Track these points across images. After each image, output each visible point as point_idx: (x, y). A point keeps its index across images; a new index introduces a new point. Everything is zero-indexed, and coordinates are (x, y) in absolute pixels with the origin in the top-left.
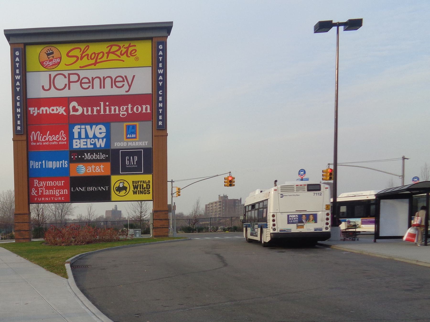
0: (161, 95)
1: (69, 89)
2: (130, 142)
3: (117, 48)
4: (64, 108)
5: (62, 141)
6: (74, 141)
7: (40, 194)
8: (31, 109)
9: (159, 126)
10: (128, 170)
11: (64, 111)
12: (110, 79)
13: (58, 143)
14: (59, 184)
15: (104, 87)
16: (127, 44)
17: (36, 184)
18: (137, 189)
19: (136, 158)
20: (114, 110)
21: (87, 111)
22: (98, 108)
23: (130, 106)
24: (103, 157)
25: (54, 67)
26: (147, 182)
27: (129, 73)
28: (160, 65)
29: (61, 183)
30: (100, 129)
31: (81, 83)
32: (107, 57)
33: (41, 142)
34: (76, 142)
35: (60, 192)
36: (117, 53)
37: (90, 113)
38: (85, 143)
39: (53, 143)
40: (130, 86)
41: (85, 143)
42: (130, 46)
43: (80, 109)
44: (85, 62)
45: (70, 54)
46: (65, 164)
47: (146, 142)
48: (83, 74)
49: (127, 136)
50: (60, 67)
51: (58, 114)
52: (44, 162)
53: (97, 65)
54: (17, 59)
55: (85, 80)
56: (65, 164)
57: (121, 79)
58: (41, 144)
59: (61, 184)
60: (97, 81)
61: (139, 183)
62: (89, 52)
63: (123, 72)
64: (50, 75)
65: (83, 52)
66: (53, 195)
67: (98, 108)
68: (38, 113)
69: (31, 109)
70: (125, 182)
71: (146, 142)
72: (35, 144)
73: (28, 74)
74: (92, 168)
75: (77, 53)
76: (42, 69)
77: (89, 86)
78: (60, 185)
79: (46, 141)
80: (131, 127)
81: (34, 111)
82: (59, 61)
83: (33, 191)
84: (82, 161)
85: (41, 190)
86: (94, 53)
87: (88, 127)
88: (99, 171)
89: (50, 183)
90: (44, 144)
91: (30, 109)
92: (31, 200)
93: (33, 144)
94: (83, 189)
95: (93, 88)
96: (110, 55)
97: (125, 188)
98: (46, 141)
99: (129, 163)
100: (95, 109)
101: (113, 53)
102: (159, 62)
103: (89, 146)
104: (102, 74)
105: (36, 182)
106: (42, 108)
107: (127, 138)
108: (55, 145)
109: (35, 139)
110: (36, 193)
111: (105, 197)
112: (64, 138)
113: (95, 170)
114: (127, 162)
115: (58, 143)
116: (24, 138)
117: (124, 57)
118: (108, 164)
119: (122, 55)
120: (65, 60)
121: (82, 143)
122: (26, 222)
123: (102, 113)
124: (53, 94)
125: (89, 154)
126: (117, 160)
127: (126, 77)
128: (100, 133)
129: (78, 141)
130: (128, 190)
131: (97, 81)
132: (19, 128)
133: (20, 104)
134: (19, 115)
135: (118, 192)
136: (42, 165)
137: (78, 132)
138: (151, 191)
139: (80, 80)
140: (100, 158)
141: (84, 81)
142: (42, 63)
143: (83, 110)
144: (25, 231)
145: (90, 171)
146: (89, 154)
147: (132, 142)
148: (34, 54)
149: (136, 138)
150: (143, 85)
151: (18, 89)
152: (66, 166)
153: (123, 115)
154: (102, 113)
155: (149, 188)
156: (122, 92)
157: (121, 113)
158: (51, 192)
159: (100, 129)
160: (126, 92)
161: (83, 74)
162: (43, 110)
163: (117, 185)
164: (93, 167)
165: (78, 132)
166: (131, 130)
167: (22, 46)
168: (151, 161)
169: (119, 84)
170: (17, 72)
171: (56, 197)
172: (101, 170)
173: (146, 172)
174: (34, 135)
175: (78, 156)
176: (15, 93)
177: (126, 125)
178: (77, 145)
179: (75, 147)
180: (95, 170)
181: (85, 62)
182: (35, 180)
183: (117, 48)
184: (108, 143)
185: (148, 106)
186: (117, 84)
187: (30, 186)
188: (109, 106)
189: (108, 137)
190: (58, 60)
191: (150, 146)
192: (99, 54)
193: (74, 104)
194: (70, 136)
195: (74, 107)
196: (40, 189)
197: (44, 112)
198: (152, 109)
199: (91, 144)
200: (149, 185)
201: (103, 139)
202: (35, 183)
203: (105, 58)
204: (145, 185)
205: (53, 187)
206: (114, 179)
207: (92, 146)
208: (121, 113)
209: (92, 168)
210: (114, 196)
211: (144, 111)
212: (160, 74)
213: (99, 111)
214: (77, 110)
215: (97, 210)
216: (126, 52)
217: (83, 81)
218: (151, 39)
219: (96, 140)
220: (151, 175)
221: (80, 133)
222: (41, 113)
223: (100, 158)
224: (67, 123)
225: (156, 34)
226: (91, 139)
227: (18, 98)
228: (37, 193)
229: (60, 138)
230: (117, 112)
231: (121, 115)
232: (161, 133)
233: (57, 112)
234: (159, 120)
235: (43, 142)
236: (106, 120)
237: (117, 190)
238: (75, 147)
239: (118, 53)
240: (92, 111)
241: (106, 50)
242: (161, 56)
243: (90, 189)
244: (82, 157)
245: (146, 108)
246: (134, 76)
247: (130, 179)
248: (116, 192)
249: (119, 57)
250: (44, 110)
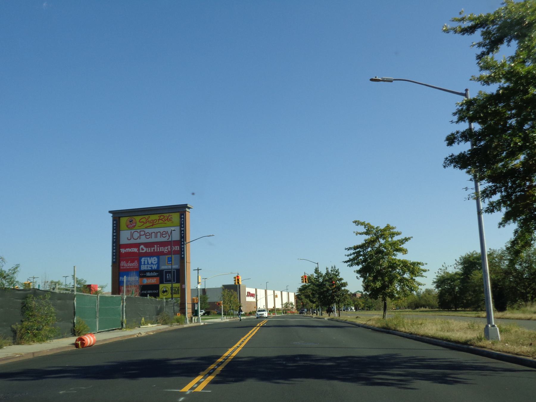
8: (121, 250)
10: (168, 281)
16: (167, 215)
20: (162, 249)
23: (169, 247)
24: (155, 274)
42: (169, 216)
44: (148, 224)
45: (141, 221)
48: (147, 231)
50: (136, 228)
55: (148, 234)
60: (153, 235)
62: (150, 220)
63: (166, 229)
69: (121, 250)
76: (127, 228)
87: (149, 258)
97: (166, 291)
101: (161, 219)
114: (168, 277)
117: (166, 222)
118: (158, 278)
120: (139, 224)
124: (132, 241)
131: (153, 235)
142: (127, 226)
148: (124, 221)
169: (164, 236)
173: (177, 282)
174: (123, 264)
175: (142, 274)
176: (113, 242)
181: (148, 224)
184: (158, 267)
189: (158, 263)
193: (142, 246)
206: (161, 286)
213: (154, 250)
221: (144, 262)
224: (138, 256)
225: (181, 210)
236: (158, 254)
238: (142, 269)
240: (151, 250)
241: (158, 218)
247: (169, 286)
250: (129, 250)
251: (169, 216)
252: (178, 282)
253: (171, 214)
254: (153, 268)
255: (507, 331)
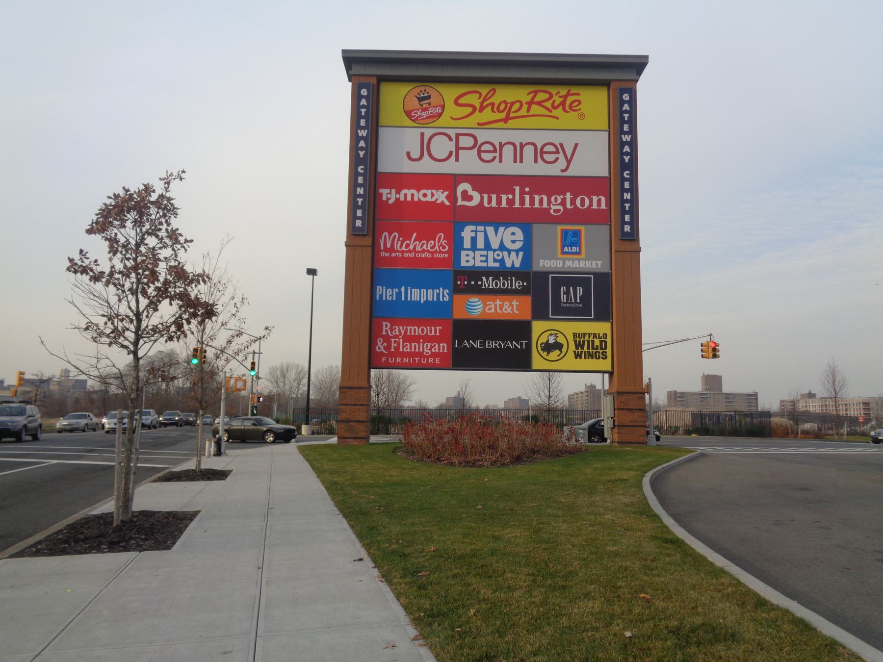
0: (627, 180)
1: (457, 159)
2: (569, 259)
3: (546, 96)
4: (446, 193)
5: (440, 252)
6: (463, 253)
7: (393, 350)
8: (384, 192)
9: (624, 233)
11: (447, 197)
12: (532, 147)
13: (433, 256)
14: (431, 332)
15: (521, 161)
16: (563, 91)
17: (386, 331)
18: (582, 348)
19: (580, 291)
20: (540, 201)
21: (490, 201)
22: (511, 197)
23: (568, 196)
24: (517, 284)
25: (430, 120)
26: (601, 335)
27: (568, 140)
28: (626, 128)
29: (435, 330)
30: (513, 234)
31: (479, 152)
32: (528, 111)
33: (399, 252)
34: (467, 255)
35: (431, 347)
36: (545, 104)
37: (494, 204)
38: (484, 259)
39: (423, 255)
40: (569, 162)
41: (484, 259)
42: (568, 94)
43: (476, 196)
45: (460, 101)
46: (444, 296)
47: (600, 263)
48: (483, 135)
49: (563, 248)
51: (434, 203)
52: (403, 289)
53: (510, 121)
54: (364, 102)
55: (488, 147)
56: (444, 294)
57: (553, 149)
58: (399, 255)
59: (435, 332)
60: (508, 151)
61: (587, 338)
62: (496, 99)
63: (556, 138)
64: (422, 135)
65: (485, 100)
66: (419, 352)
67: (511, 197)
68: (397, 200)
69: (384, 192)
70: (560, 335)
71: (600, 263)
72: (387, 255)
73: (381, 130)
74: (496, 305)
75: (474, 99)
76: (410, 123)
77: (494, 158)
78: (433, 334)
79: (410, 251)
80: (570, 234)
81: (389, 196)
82: (440, 111)
83: (379, 344)
84: (478, 290)
85: (395, 342)
86: (505, 102)
87: (490, 230)
88: (509, 310)
89: (414, 330)
90: (406, 255)
91: (381, 191)
92: (374, 361)
93: (383, 254)
94: (478, 345)
95: (501, 161)
96: (534, 107)
97: (558, 346)
98: (410, 251)
99: (567, 299)
100: (504, 197)
101: (539, 103)
102: (622, 122)
103: (492, 264)
104: (518, 137)
105: (386, 326)
106: (405, 191)
107: (563, 253)
108: (426, 258)
109: (389, 246)
110: (385, 348)
111: (520, 361)
112: (444, 248)
113: (501, 309)
114: (563, 298)
115: (433, 256)
116: (368, 241)
117: (559, 112)
118: (527, 300)
119: (555, 108)
120: (451, 110)
121: (478, 258)
122: (362, 405)
123: (517, 205)
124: (427, 166)
125: (491, 278)
126: (545, 292)
127: (561, 145)
128: (513, 242)
129: (471, 253)
130: (564, 349)
131: (508, 151)
132: (359, 223)
133: (364, 180)
134: (360, 200)
135: (546, 353)
136: (399, 294)
137: (472, 238)
138: (609, 354)
139: (477, 147)
140: (512, 286)
141: (484, 148)
142: (408, 114)
143: (482, 198)
144: (359, 421)
145: (493, 311)
146: (491, 278)
147: (573, 260)
148: (395, 97)
149: (579, 253)
150: (592, 159)
151: (362, 153)
152: (447, 299)
153: (556, 211)
154: (517, 205)
155: (606, 348)
156: (554, 170)
157: (553, 207)
158: (414, 347)
159: (513, 234)
160: (562, 171)
161: (483, 135)
162: (406, 195)
163: (543, 339)
164: (498, 303)
165: (472, 238)
166: (571, 240)
167: (374, 81)
168: (609, 296)
170: (363, 122)
171: (424, 357)
172: (512, 310)
173: (598, 319)
174: (387, 239)
175: (470, 281)
176: (355, 161)
177: (562, 230)
178: (467, 261)
179: (464, 264)
180: (501, 309)
181: (488, 115)
182: (384, 323)
183: (546, 96)
185: (603, 199)
186: (545, 156)
187: (373, 334)
188: (531, 194)
189: (527, 249)
190: (439, 110)
191: (607, 270)
192: (513, 103)
194: (456, 245)
195: (465, 193)
196: (393, 340)
197: (409, 199)
198: (608, 203)
199: (495, 261)
200: (606, 343)
201: (517, 251)
202: (384, 329)
203: (523, 112)
204: (597, 342)
205: (420, 337)
206: (538, 327)
207: (497, 265)
208: (553, 207)
209: (496, 305)
210: (537, 360)
211: (595, 206)
212: (626, 143)
213: (511, 202)
214: (470, 198)
215: (491, 389)
216: (563, 104)
217: (483, 148)
218: (606, 84)
219: (505, 253)
220: (609, 324)
221: (474, 240)
222: (402, 199)
223: (512, 286)
226: (494, 251)
227: (360, 169)
228: (388, 348)
229: (435, 246)
230: (545, 205)
231: (552, 211)
232: (627, 246)
233: (433, 199)
234: (624, 223)
235: (403, 252)
236: (525, 220)
237: (543, 349)
238: (464, 264)
239: (548, 104)
240: (499, 201)
241: (527, 99)
242: (626, 111)
243: (492, 344)
244: (476, 283)
245: (599, 201)
246: (576, 145)
247: (568, 329)
248: (541, 352)
249: (551, 111)
251: (568, 94)
252: (603, 315)
253: (574, 90)
254: (508, 264)
255: (534, 452)
